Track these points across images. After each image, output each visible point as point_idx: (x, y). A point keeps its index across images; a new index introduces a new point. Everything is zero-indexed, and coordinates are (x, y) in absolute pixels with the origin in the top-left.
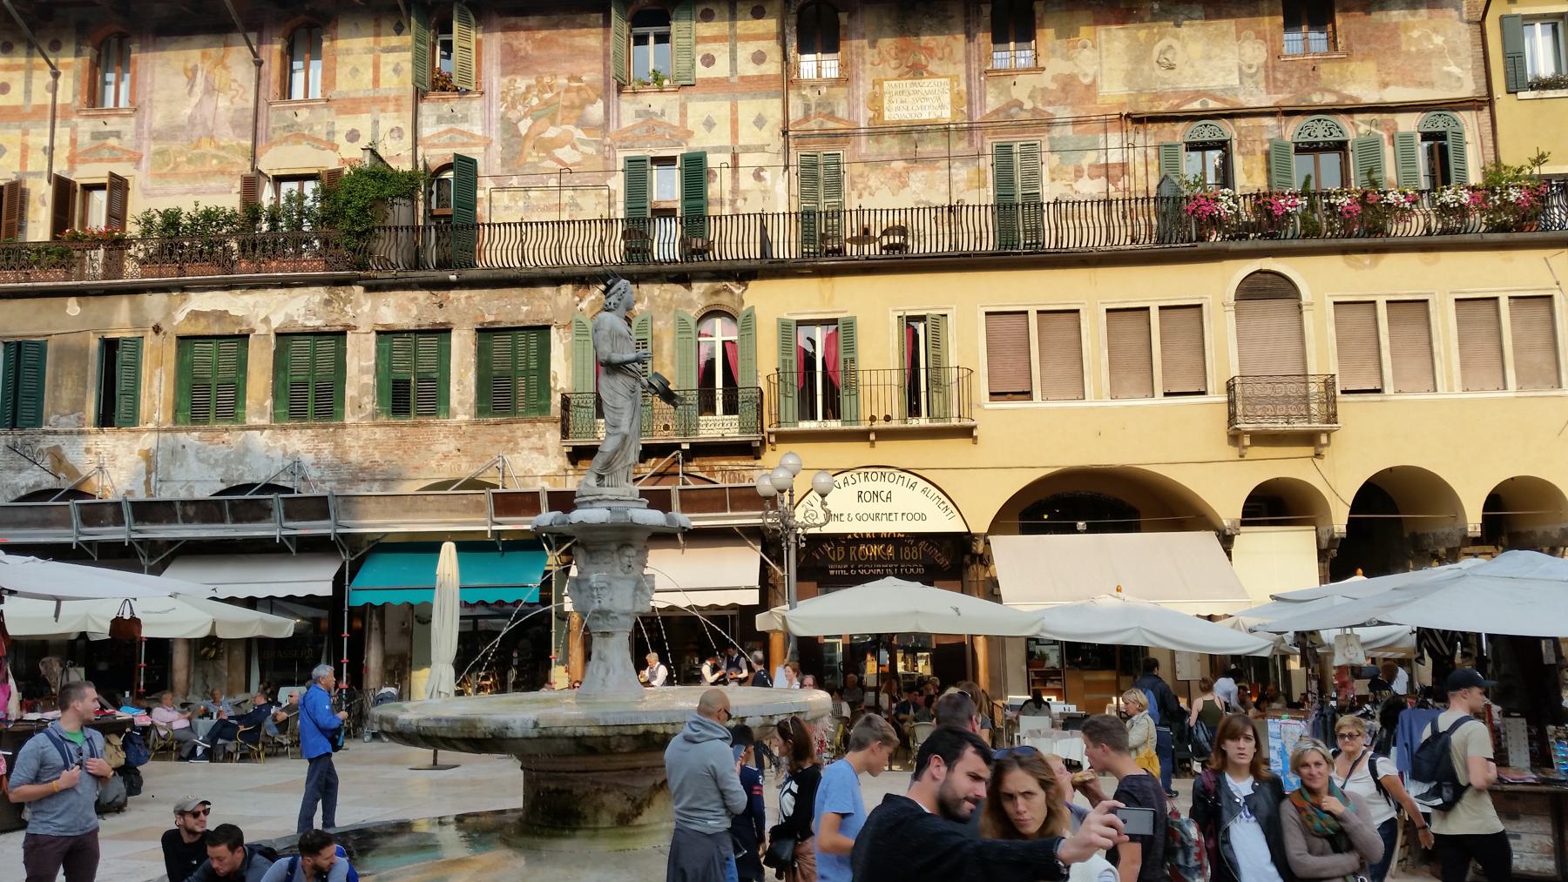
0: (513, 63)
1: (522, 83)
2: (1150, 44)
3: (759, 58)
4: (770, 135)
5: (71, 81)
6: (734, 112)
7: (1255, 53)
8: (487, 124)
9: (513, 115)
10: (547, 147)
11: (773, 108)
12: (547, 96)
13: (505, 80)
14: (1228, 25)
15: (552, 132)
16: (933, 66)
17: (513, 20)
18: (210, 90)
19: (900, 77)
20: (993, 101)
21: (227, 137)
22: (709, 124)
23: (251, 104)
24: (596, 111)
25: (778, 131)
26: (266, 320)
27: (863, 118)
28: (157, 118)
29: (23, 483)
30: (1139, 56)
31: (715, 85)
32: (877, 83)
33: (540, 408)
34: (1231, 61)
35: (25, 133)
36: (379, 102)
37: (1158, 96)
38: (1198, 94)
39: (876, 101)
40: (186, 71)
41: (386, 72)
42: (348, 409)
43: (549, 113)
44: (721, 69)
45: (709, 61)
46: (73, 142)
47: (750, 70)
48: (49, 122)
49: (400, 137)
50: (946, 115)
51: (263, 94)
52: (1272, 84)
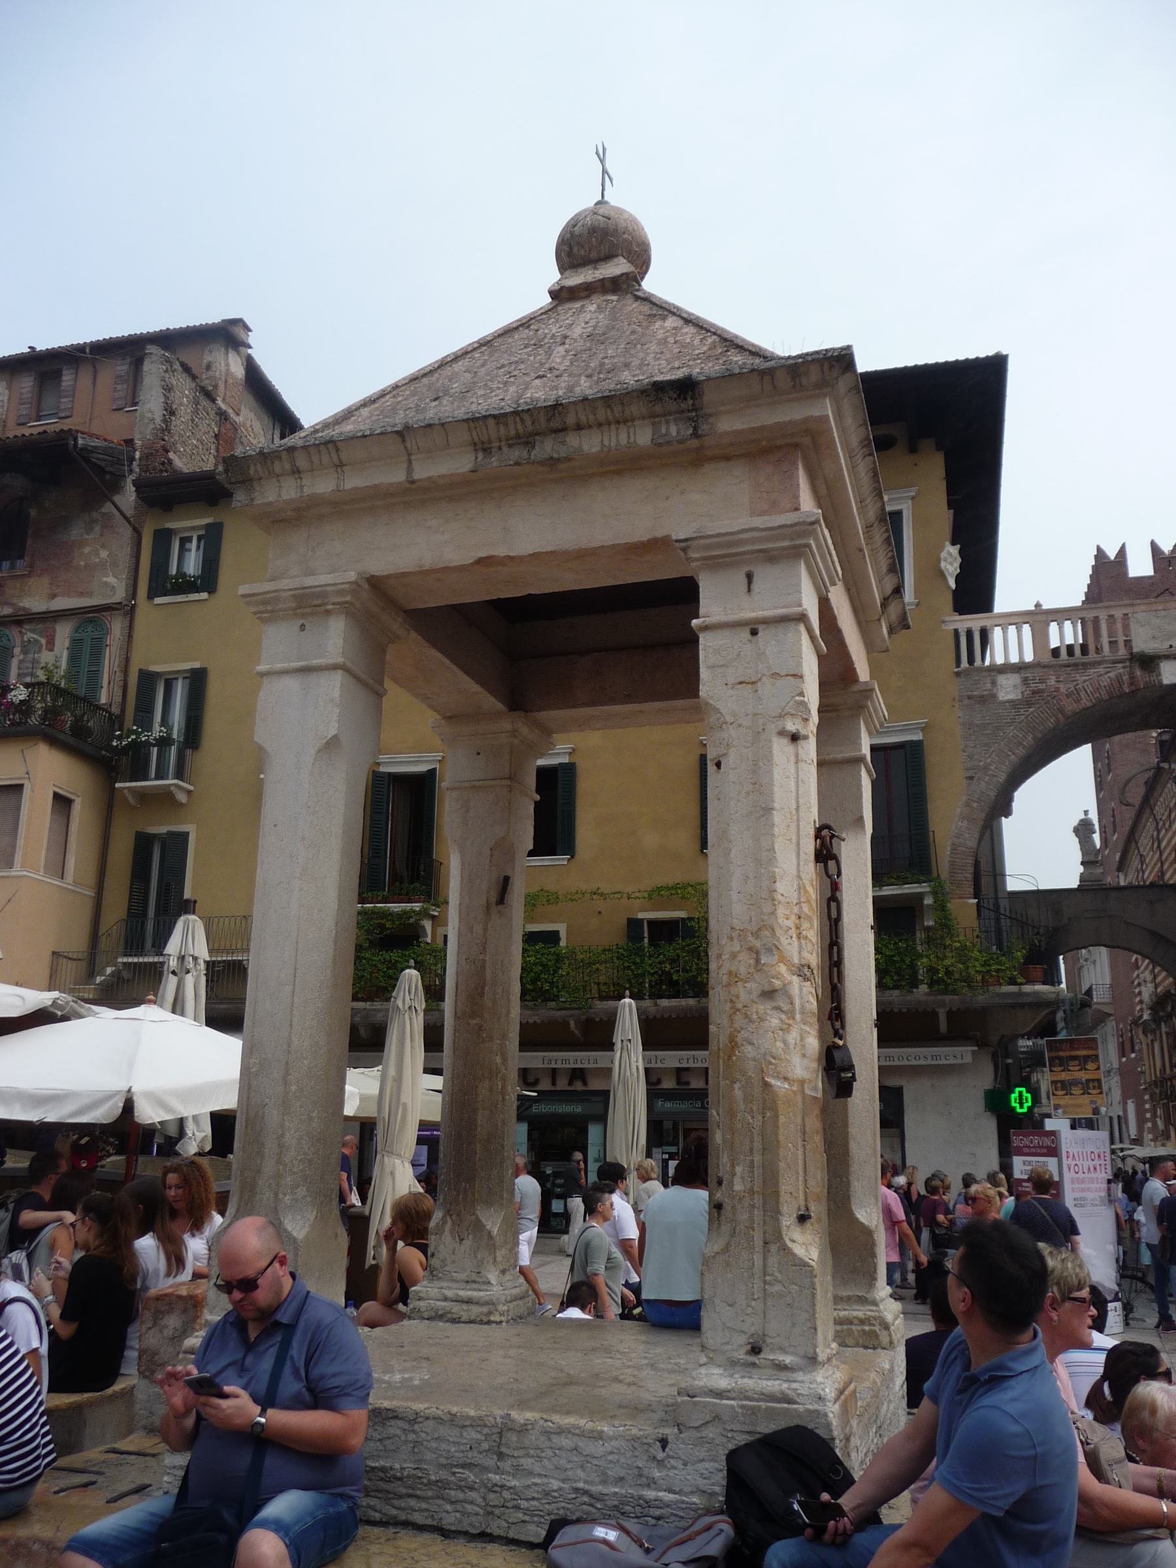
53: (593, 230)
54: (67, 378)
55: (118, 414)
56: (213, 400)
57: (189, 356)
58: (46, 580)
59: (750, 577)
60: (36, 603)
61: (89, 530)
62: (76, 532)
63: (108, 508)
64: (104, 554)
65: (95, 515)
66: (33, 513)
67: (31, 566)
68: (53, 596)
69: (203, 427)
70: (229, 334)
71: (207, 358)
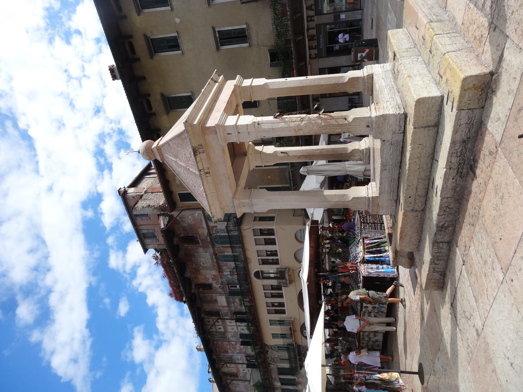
0: (226, 352)
1: (229, 351)
2: (202, 266)
3: (219, 322)
7: (201, 250)
10: (241, 349)
11: (227, 321)
14: (196, 254)
15: (238, 348)
16: (215, 298)
18: (238, 385)
20: (220, 290)
22: (232, 329)
24: (233, 343)
27: (226, 308)
30: (206, 268)
31: (224, 328)
32: (219, 306)
34: (203, 254)
36: (237, 368)
37: (214, 265)
38: (212, 259)
39: (223, 307)
43: (235, 349)
44: (221, 327)
45: (220, 328)
47: (221, 323)
50: (224, 297)
52: (207, 247)
53: (147, 155)
54: (144, 232)
55: (151, 218)
56: (142, 195)
57: (131, 204)
58: (199, 230)
59: (228, 134)
60: (206, 232)
61: (184, 221)
62: (185, 225)
63: (178, 218)
64: (190, 217)
65: (180, 221)
66: (182, 235)
67: (196, 234)
68: (203, 228)
69: (151, 197)
70: (123, 194)
71: (131, 198)
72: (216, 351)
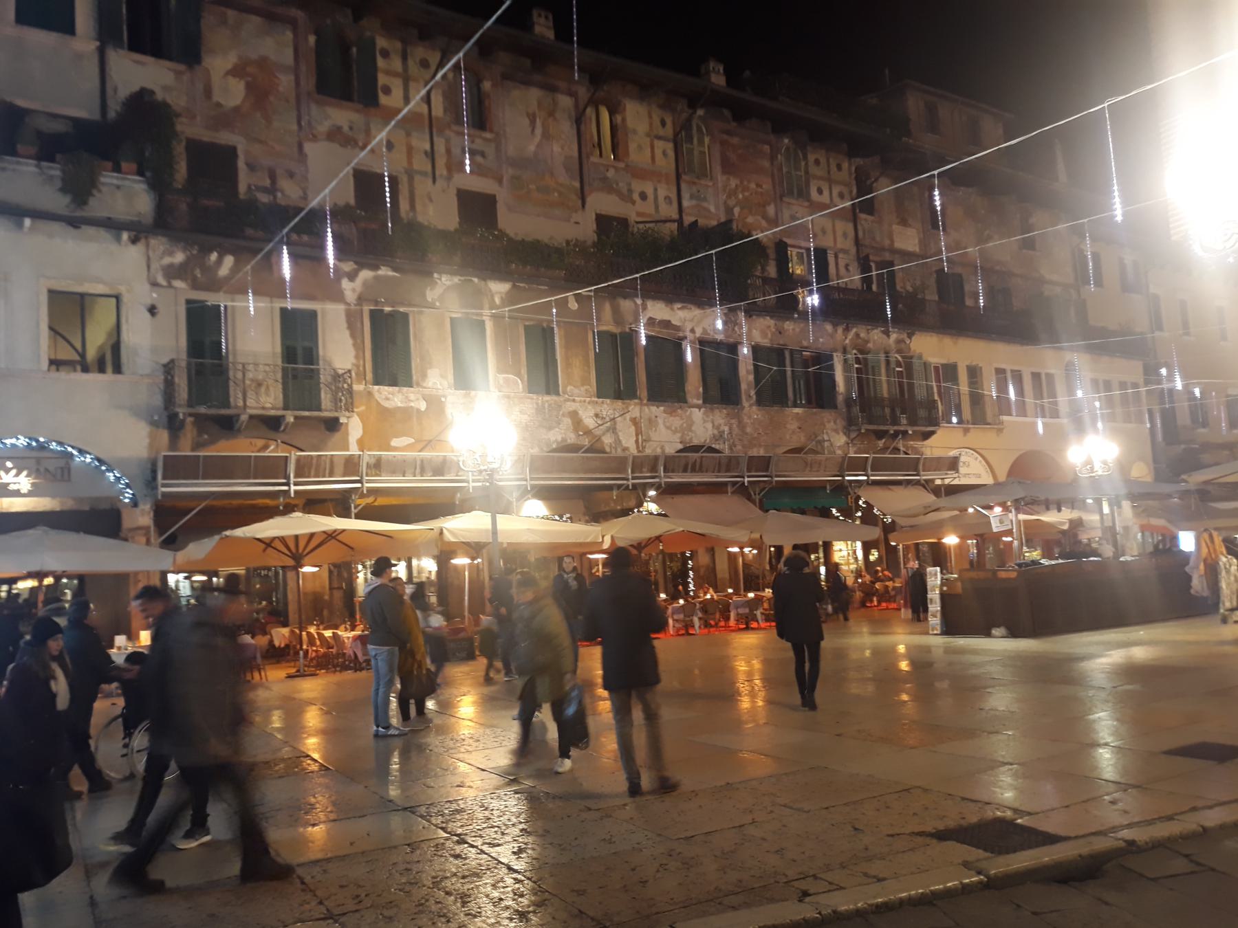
0: (728, 168)
1: (734, 182)
4: (849, 244)
5: (440, 99)
6: (834, 226)
8: (717, 208)
9: (732, 202)
12: (747, 194)
13: (725, 178)
17: (725, 137)
19: (898, 224)
21: (563, 177)
23: (576, 154)
25: (852, 242)
26: (693, 331)
28: (511, 150)
29: (553, 439)
33: (833, 406)
35: (408, 135)
40: (528, 115)
41: (658, 152)
42: (744, 397)
46: (448, 151)
48: (427, 130)
49: (671, 203)
51: (584, 150)
72: (728, 133)
